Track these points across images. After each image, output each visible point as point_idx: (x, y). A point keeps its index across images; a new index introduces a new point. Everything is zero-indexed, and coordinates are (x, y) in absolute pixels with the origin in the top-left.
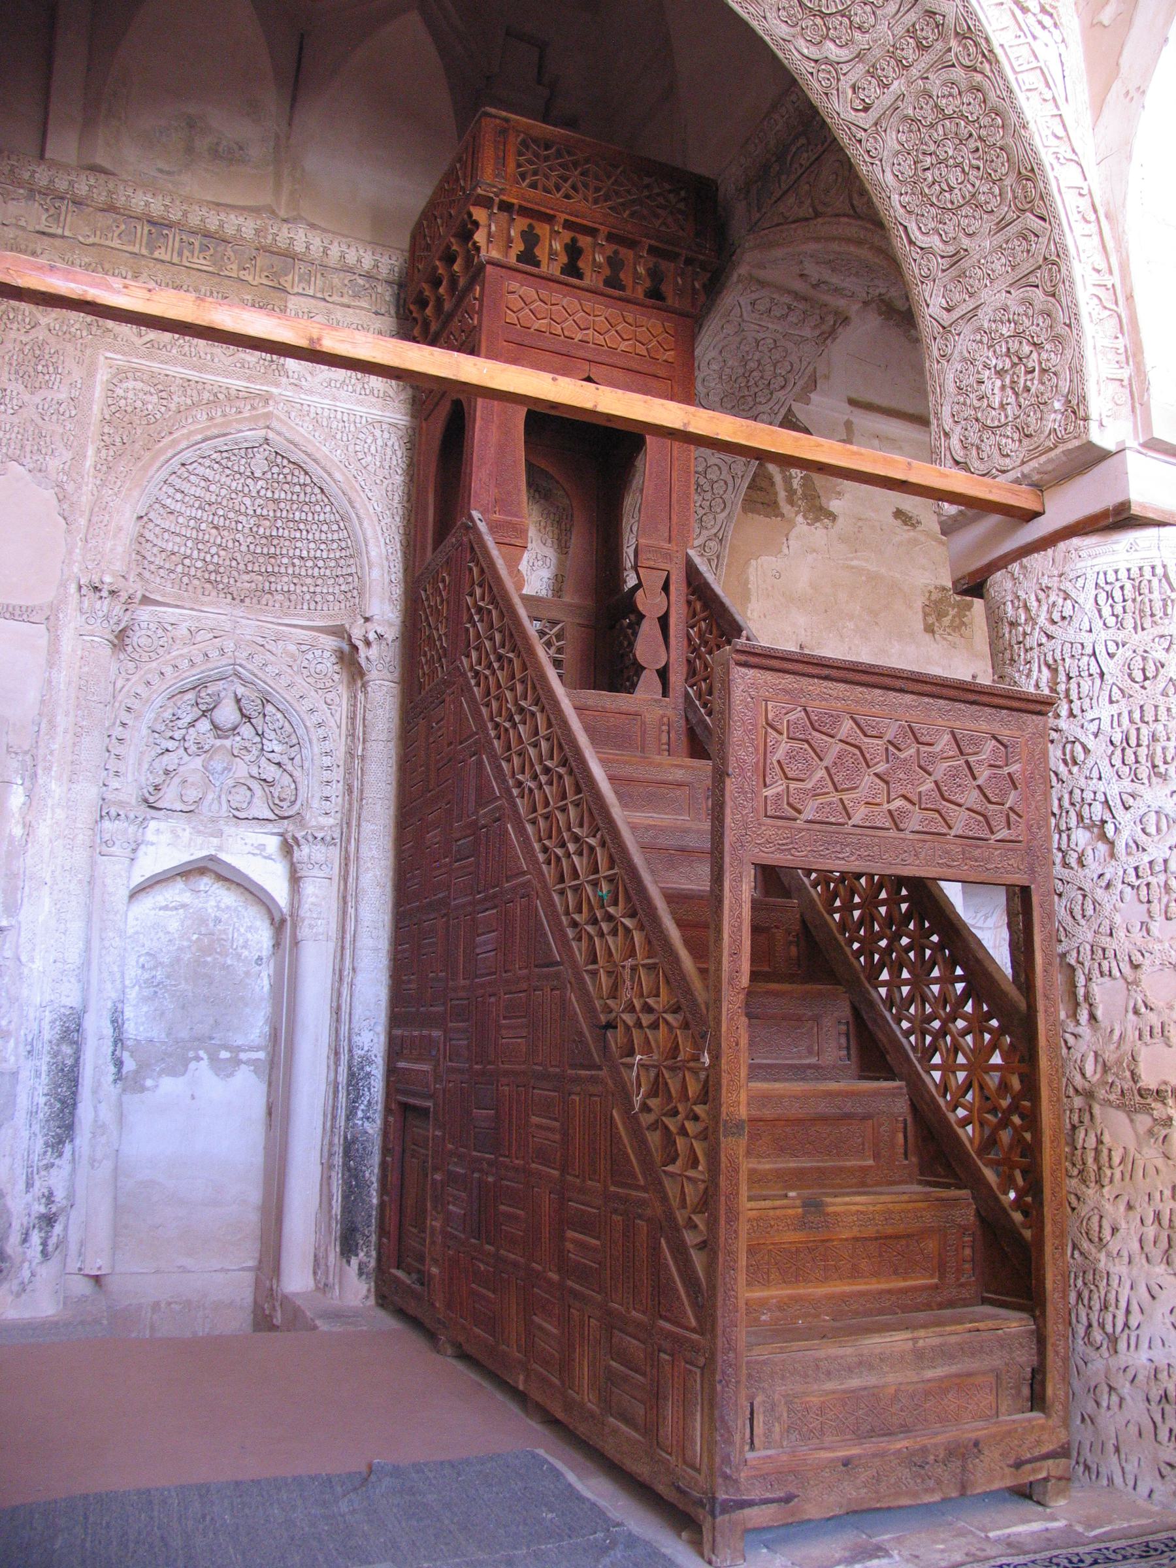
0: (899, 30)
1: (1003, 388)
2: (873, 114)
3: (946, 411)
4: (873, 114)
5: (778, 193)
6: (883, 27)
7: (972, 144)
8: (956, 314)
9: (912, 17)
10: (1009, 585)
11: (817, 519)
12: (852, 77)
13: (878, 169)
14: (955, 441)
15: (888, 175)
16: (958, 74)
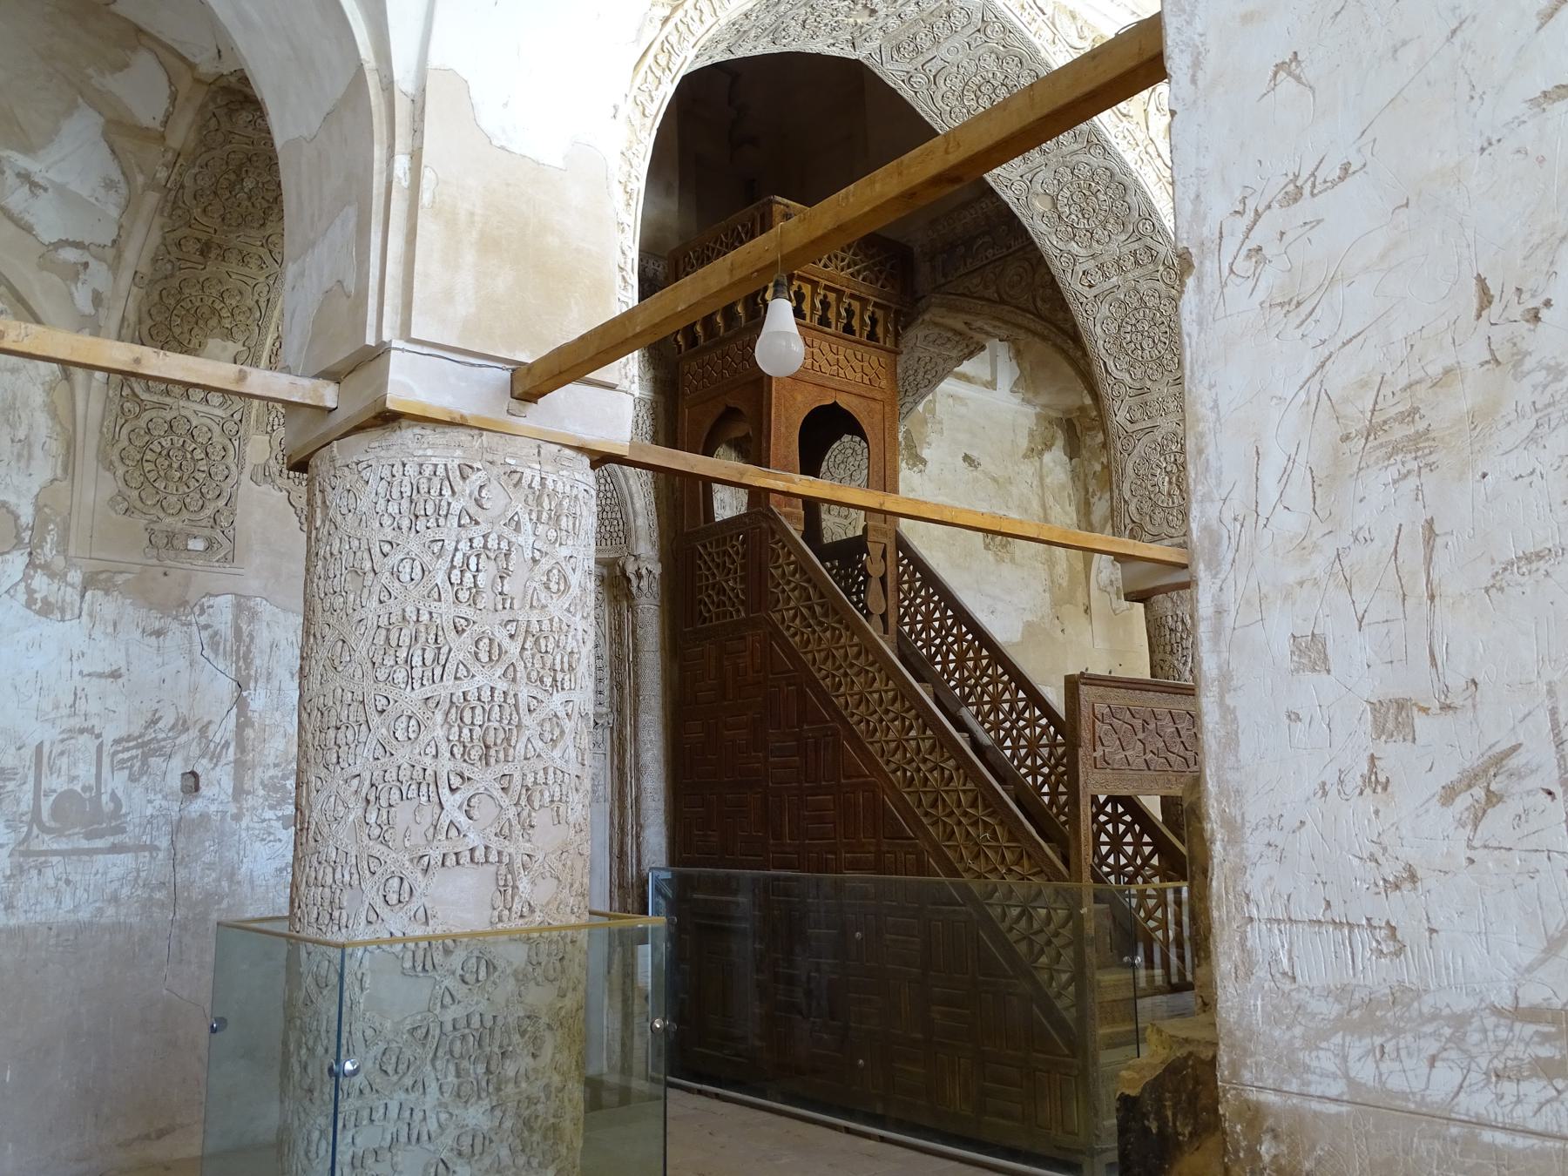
0: (1125, 250)
1: (1170, 483)
2: (1094, 291)
3: (1126, 487)
4: (1094, 291)
5: (962, 271)
6: (1114, 245)
7: (1163, 328)
8: (1137, 427)
9: (1136, 246)
10: (1169, 605)
11: (915, 465)
12: (1085, 267)
13: (1091, 323)
14: (1132, 508)
15: (1098, 330)
16: (1160, 285)
